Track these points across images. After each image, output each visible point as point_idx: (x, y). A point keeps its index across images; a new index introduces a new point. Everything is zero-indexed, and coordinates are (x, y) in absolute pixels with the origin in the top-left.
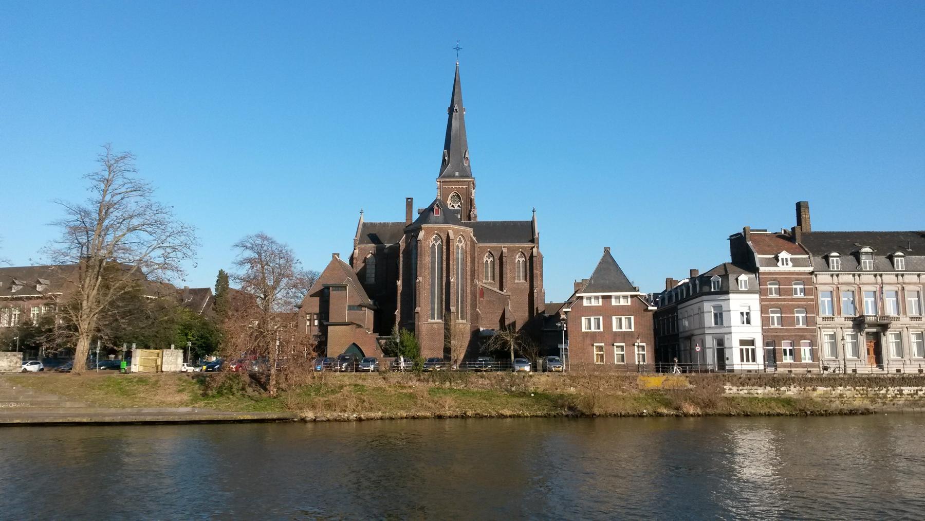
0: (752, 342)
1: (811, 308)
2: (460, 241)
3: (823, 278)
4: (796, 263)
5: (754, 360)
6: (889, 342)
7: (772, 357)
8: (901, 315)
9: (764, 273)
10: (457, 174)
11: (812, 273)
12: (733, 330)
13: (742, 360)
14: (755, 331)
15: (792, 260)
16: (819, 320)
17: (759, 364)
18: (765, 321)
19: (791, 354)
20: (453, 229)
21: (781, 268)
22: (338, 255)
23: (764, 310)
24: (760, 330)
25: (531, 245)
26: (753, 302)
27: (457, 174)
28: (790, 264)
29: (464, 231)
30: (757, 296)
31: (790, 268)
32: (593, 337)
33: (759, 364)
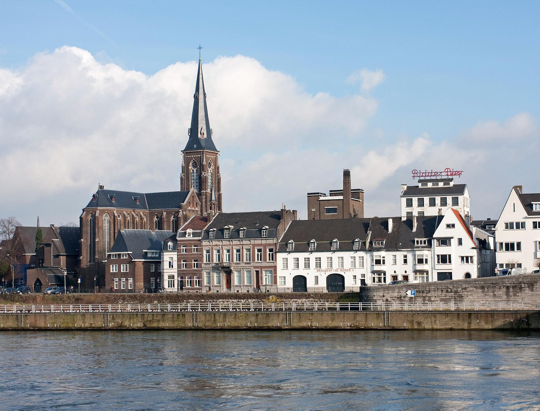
0: (173, 277)
1: (199, 259)
2: (106, 216)
3: (204, 243)
4: (194, 235)
5: (174, 287)
6: (235, 276)
7: (182, 285)
8: (251, 261)
9: (180, 241)
10: (195, 146)
11: (200, 240)
12: (165, 271)
13: (169, 287)
14: (174, 271)
15: (193, 233)
16: (203, 265)
17: (175, 289)
18: (179, 266)
19: (199, 283)
20: (100, 210)
21: (187, 237)
22: (53, 225)
23: (179, 260)
24: (176, 271)
25: (176, 209)
26: (174, 255)
27: (195, 146)
28: (191, 236)
29: (107, 210)
30: (176, 253)
31: (191, 238)
32: (114, 275)
33: (175, 289)
